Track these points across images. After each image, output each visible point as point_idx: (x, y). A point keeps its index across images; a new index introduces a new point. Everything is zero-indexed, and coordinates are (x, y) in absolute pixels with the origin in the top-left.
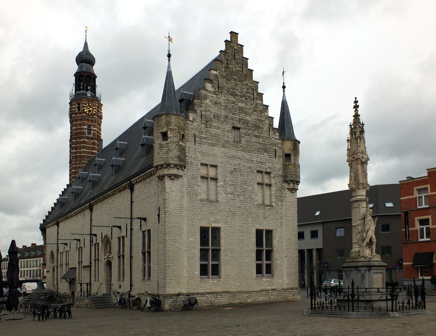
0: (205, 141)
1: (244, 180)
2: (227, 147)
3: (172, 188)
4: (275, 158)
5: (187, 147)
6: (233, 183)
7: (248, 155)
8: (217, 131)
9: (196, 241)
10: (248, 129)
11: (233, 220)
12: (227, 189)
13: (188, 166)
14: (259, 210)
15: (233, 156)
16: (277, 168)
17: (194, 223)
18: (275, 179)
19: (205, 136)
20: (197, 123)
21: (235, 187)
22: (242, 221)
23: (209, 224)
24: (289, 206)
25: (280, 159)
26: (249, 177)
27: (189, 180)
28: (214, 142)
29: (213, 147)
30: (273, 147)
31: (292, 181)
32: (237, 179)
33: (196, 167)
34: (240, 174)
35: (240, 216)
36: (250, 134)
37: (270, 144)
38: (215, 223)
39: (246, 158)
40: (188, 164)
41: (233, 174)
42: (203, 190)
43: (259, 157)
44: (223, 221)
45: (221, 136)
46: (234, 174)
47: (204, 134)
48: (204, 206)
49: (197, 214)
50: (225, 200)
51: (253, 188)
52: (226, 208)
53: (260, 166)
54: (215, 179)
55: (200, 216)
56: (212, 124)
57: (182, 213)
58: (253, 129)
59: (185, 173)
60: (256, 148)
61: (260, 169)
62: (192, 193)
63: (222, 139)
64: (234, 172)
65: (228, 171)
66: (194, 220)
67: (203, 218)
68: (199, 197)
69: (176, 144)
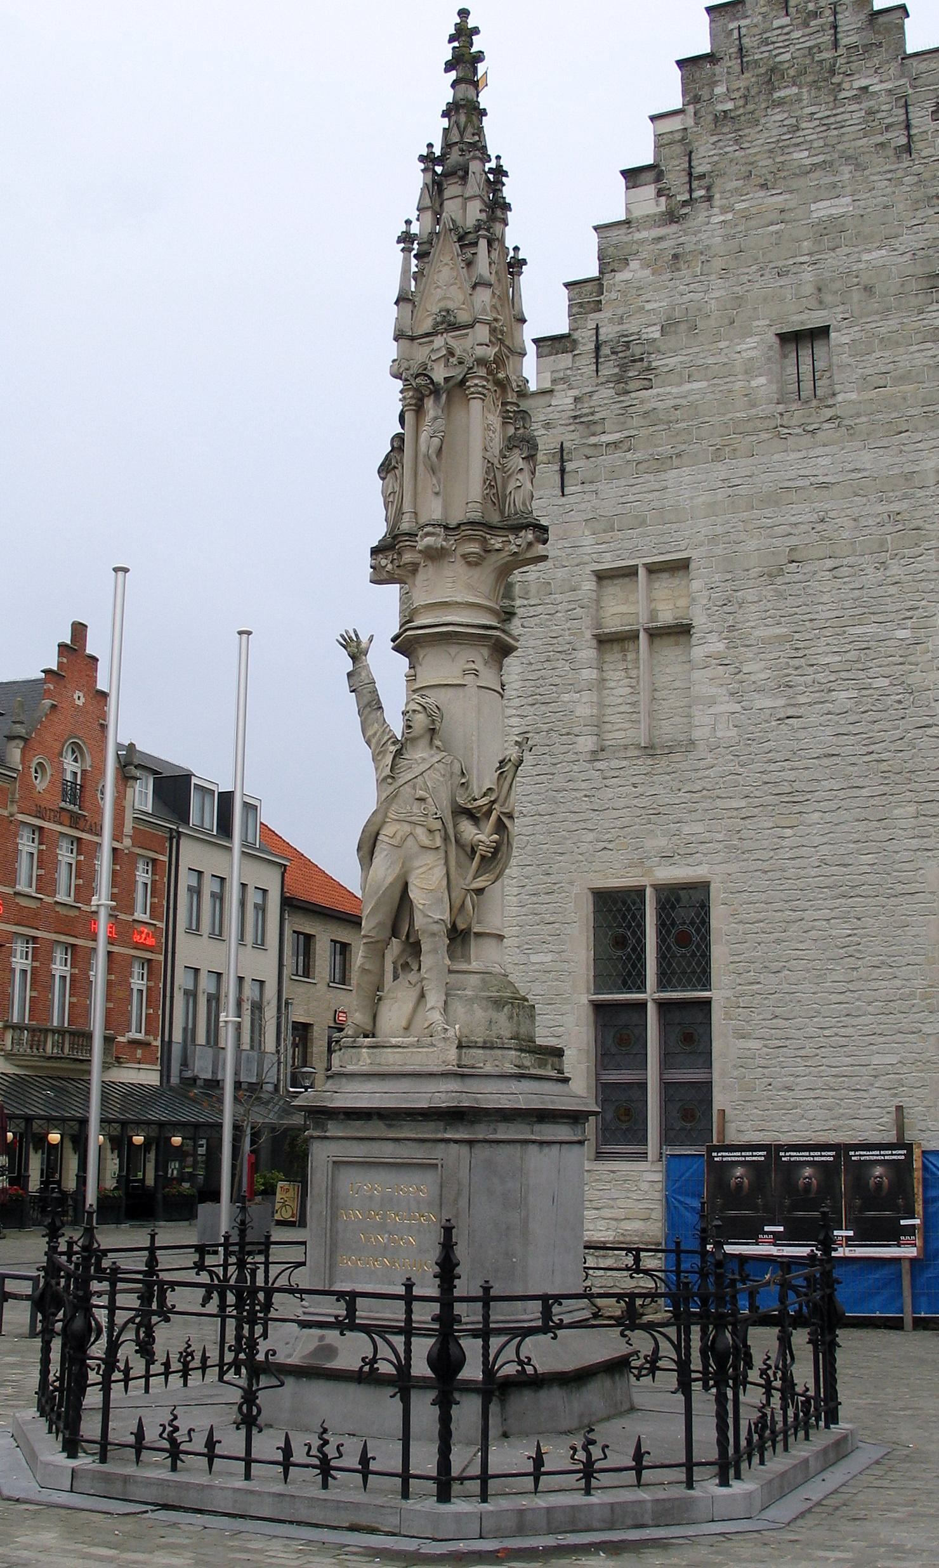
6: (779, 630)
8: (687, 387)
9: (566, 966)
10: (877, 318)
11: (788, 832)
13: (526, 602)
21: (801, 645)
23: (638, 871)
27: (533, 667)
28: (666, 449)
29: (663, 476)
35: (833, 805)
38: (671, 861)
40: (527, 593)
41: (779, 580)
42: (620, 700)
44: (720, 846)
48: (607, 782)
55: (591, 836)
65: (753, 573)
67: (603, 845)
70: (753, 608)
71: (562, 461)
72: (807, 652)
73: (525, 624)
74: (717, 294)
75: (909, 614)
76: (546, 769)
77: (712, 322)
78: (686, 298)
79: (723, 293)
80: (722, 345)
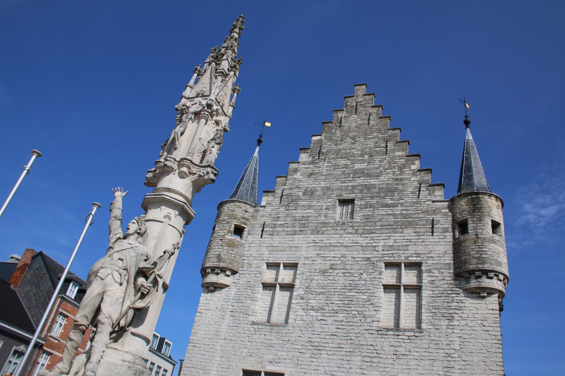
0: (280, 229)
1: (351, 282)
2: (321, 232)
3: (207, 305)
4: (431, 234)
5: (248, 242)
7: (365, 238)
10: (370, 198)
11: (315, 360)
12: (310, 301)
14: (383, 340)
15: (332, 244)
16: (438, 252)
17: (231, 363)
18: (431, 274)
19: (283, 222)
20: (273, 208)
21: (328, 296)
22: (334, 361)
23: (260, 366)
24: (473, 328)
25: (446, 234)
26: (364, 276)
27: (240, 290)
28: (297, 229)
29: (294, 236)
30: (428, 216)
31: (472, 272)
32: (334, 282)
33: (257, 269)
34: (343, 273)
35: (332, 353)
36: (375, 204)
37: (421, 212)
38: (272, 364)
39: (360, 244)
40: (243, 266)
41: (326, 274)
43: (392, 238)
44: (290, 361)
45: (312, 218)
46: (328, 274)
47: (282, 220)
49: (241, 346)
50: (301, 322)
51: (372, 295)
52: (302, 336)
53: (393, 254)
54: (289, 287)
55: (246, 350)
56: (299, 204)
57: (215, 344)
58: (382, 195)
59: (236, 281)
60: (386, 223)
61: (393, 259)
62: (240, 311)
63: (314, 222)
64: (331, 271)
65: (318, 271)
66: (234, 356)
67: (250, 354)
68: (250, 317)
69: (220, 239)
70: (316, 282)
71: (263, 227)
72: (331, 299)
73: (241, 276)
74: (322, 185)
75: (367, 291)
76: (236, 325)
77: (318, 193)
78: (312, 186)
79: (324, 185)
80: (320, 200)
